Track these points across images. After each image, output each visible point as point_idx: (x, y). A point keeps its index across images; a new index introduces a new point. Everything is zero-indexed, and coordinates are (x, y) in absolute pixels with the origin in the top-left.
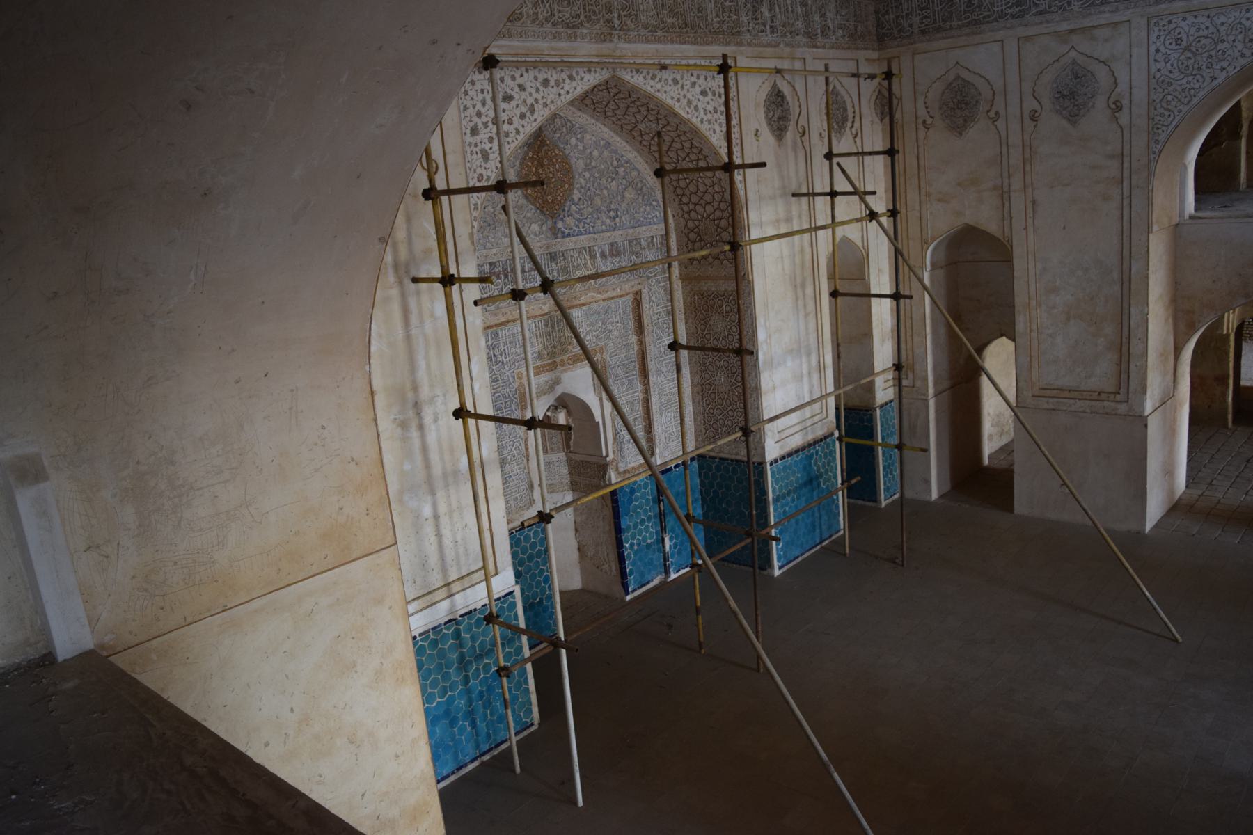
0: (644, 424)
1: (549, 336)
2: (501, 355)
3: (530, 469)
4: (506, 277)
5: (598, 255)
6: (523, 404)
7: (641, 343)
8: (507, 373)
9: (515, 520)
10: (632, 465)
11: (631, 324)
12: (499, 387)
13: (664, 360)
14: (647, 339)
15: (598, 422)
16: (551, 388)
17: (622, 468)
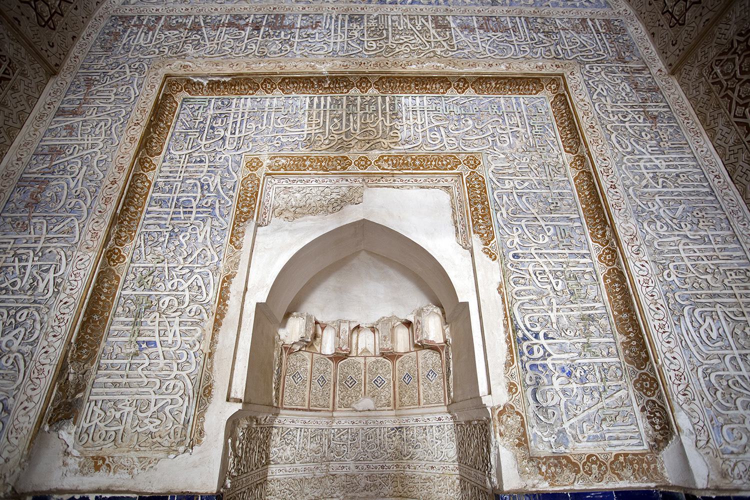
0: (621, 338)
1: (340, 117)
2: (226, 130)
3: (218, 346)
4: (257, 28)
5: (453, 25)
6: (245, 209)
7: (582, 161)
8: (227, 154)
9: (122, 467)
10: (585, 447)
11: (554, 135)
12: (202, 172)
13: (659, 193)
14: (593, 149)
15: (466, 305)
16: (338, 205)
17: (543, 444)
